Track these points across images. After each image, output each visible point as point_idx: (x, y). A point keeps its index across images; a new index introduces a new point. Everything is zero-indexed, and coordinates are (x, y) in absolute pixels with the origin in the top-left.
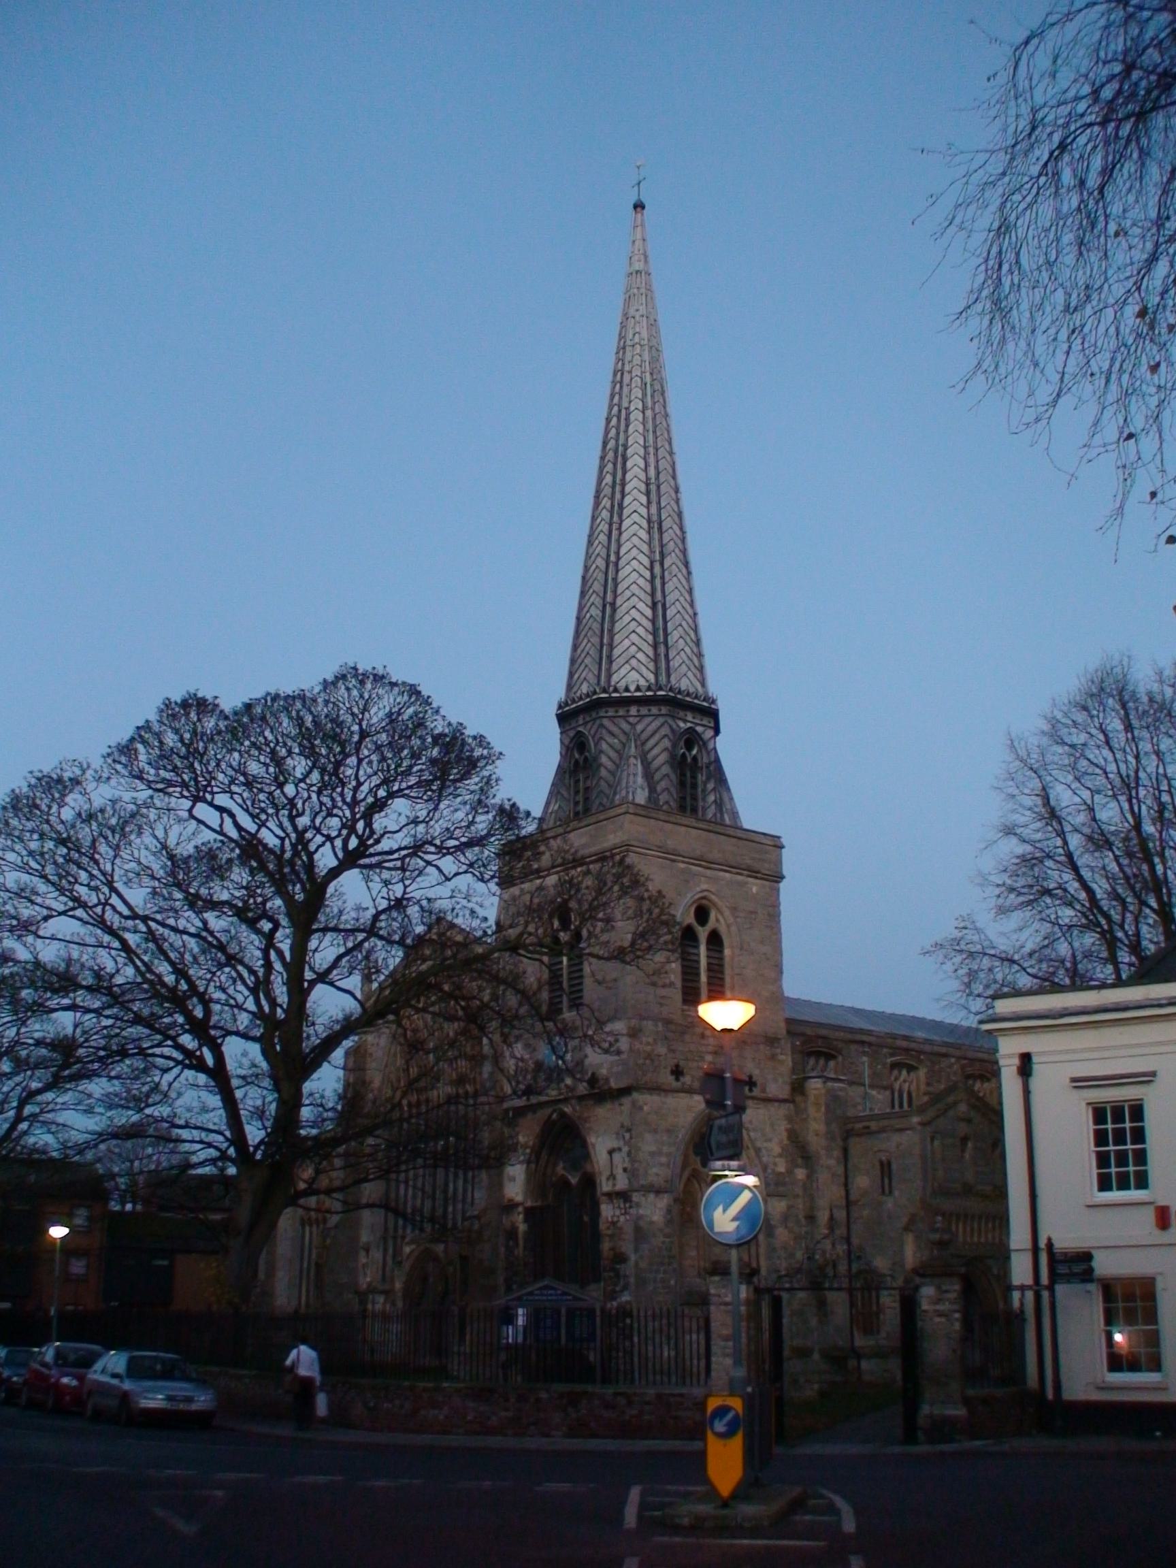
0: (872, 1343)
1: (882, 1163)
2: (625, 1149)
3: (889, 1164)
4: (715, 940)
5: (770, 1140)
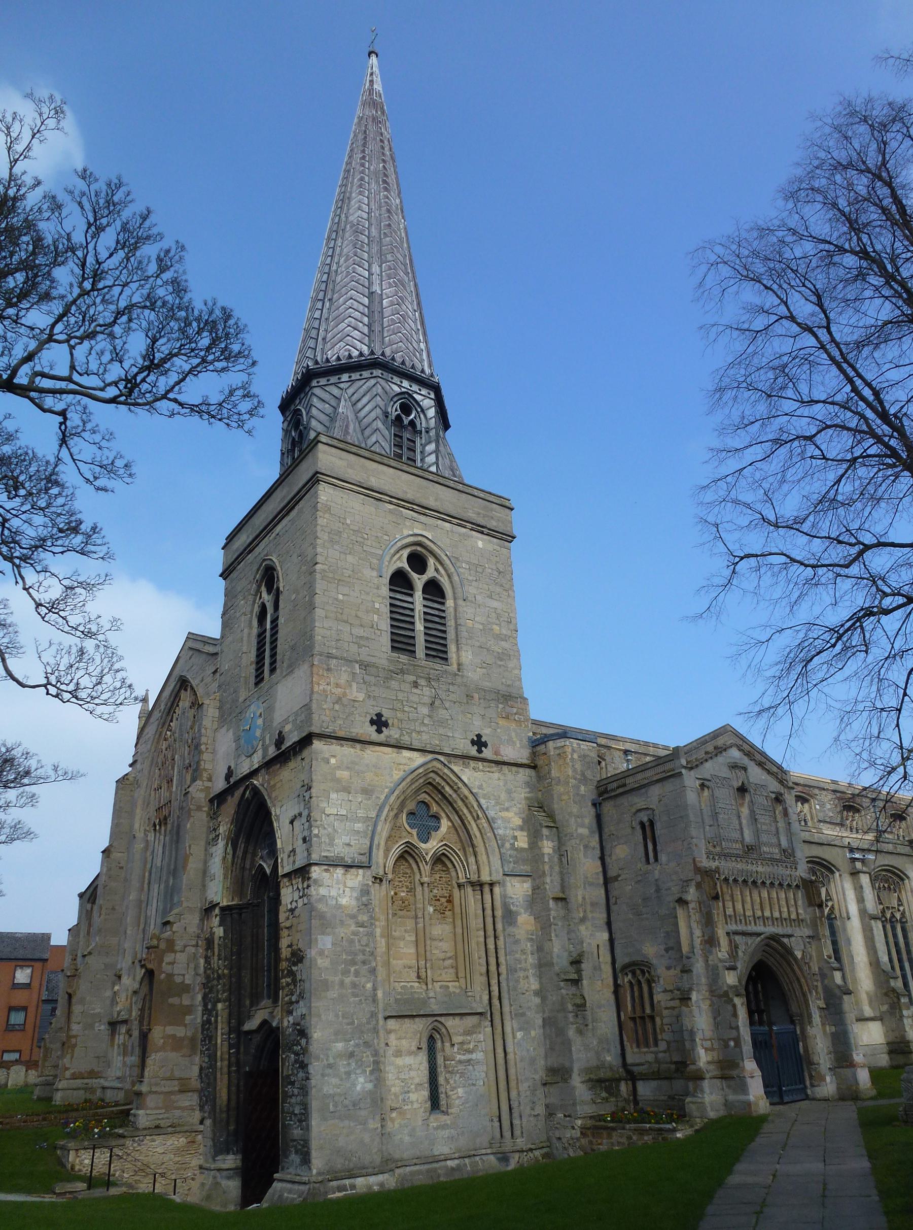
0: (650, 1058)
1: (642, 825)
2: (305, 814)
3: (652, 823)
4: (434, 589)
5: (507, 809)
